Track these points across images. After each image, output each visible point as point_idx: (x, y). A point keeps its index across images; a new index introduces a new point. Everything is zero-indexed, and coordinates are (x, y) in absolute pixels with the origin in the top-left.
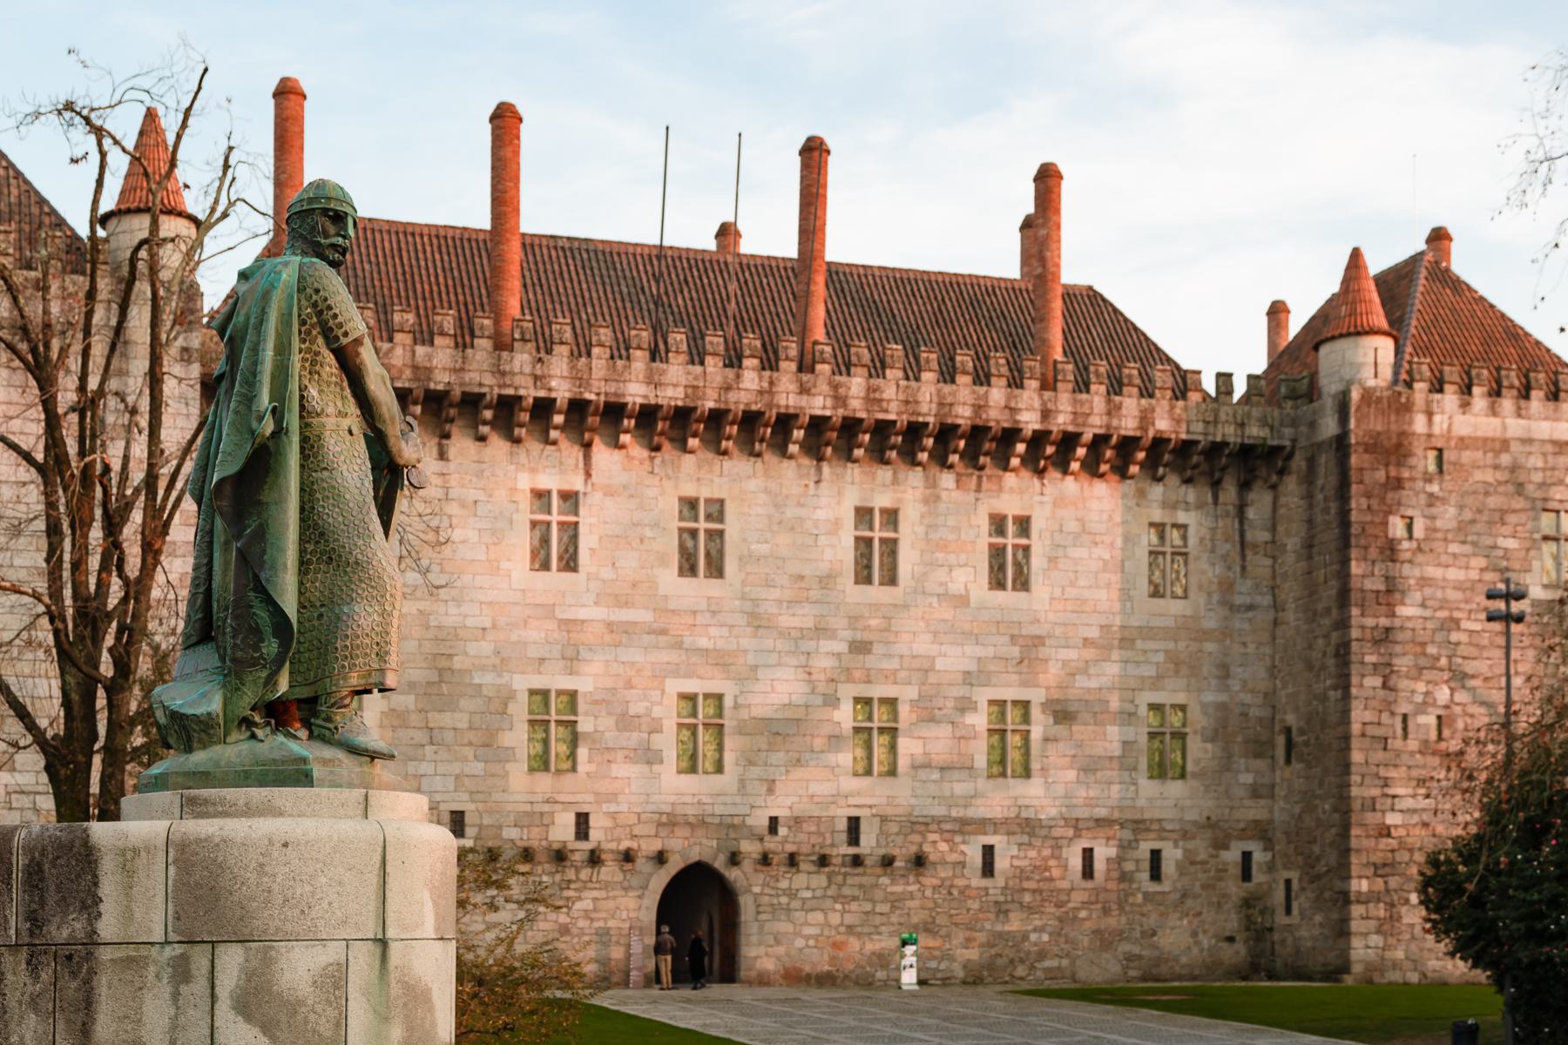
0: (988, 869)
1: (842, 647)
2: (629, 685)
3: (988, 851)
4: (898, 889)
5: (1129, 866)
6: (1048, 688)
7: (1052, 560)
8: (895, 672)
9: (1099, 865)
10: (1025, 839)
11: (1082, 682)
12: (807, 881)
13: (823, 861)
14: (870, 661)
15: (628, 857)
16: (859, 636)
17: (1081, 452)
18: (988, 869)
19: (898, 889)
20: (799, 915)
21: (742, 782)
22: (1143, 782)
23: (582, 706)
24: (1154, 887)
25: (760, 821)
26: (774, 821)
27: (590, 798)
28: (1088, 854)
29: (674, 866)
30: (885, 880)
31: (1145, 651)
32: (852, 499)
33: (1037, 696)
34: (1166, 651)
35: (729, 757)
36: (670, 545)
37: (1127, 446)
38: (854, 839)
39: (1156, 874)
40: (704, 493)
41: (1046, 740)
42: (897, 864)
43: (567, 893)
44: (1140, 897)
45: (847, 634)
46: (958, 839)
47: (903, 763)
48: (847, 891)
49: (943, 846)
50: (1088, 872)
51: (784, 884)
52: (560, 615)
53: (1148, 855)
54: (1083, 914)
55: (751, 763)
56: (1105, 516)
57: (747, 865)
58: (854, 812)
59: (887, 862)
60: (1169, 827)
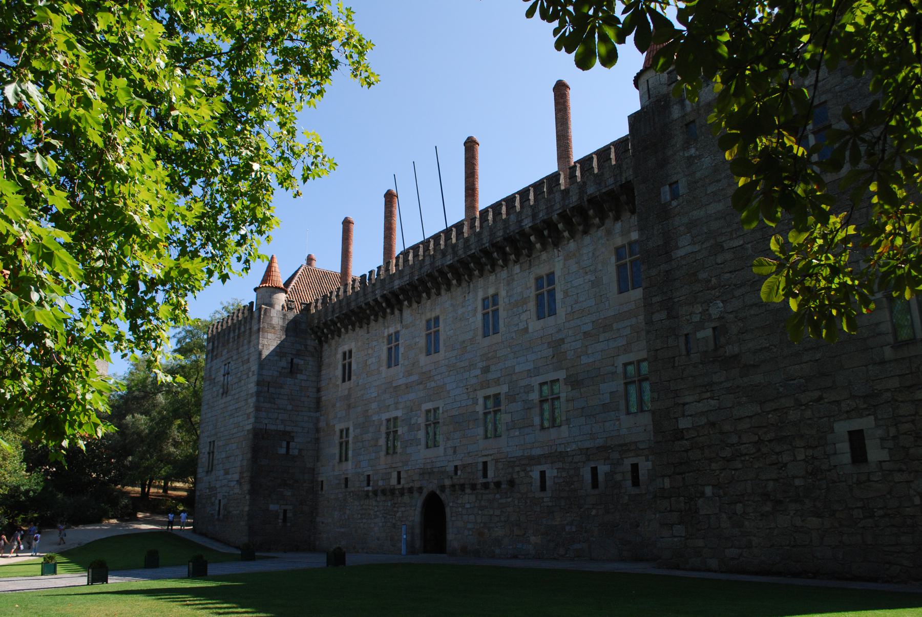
0: (543, 487)
1: (478, 372)
2: (412, 411)
3: (543, 474)
4: (503, 501)
5: (618, 477)
6: (567, 369)
7: (566, 294)
8: (498, 379)
9: (601, 477)
10: (560, 465)
11: (584, 360)
12: (468, 499)
13: (473, 487)
14: (491, 376)
15: (411, 490)
16: (484, 364)
17: (560, 226)
18: (543, 487)
19: (503, 501)
20: (465, 517)
21: (445, 449)
22: (623, 417)
23: (399, 423)
24: (634, 491)
25: (450, 468)
26: (456, 467)
27: (400, 464)
28: (594, 471)
29: (425, 492)
30: (498, 496)
31: (618, 330)
32: (481, 295)
33: (562, 375)
34: (631, 326)
35: (440, 438)
36: (422, 342)
37: (580, 210)
38: (485, 475)
39: (636, 482)
40: (433, 315)
41: (568, 401)
42: (503, 486)
43: (395, 509)
44: (627, 497)
45: (480, 365)
46: (528, 469)
47: (501, 428)
48: (483, 503)
49: (522, 474)
50: (595, 484)
51: (460, 501)
52: (394, 385)
53: (629, 468)
54: (594, 512)
55: (448, 439)
56: (591, 255)
57: (447, 491)
58: (485, 459)
59: (498, 484)
60: (641, 446)
